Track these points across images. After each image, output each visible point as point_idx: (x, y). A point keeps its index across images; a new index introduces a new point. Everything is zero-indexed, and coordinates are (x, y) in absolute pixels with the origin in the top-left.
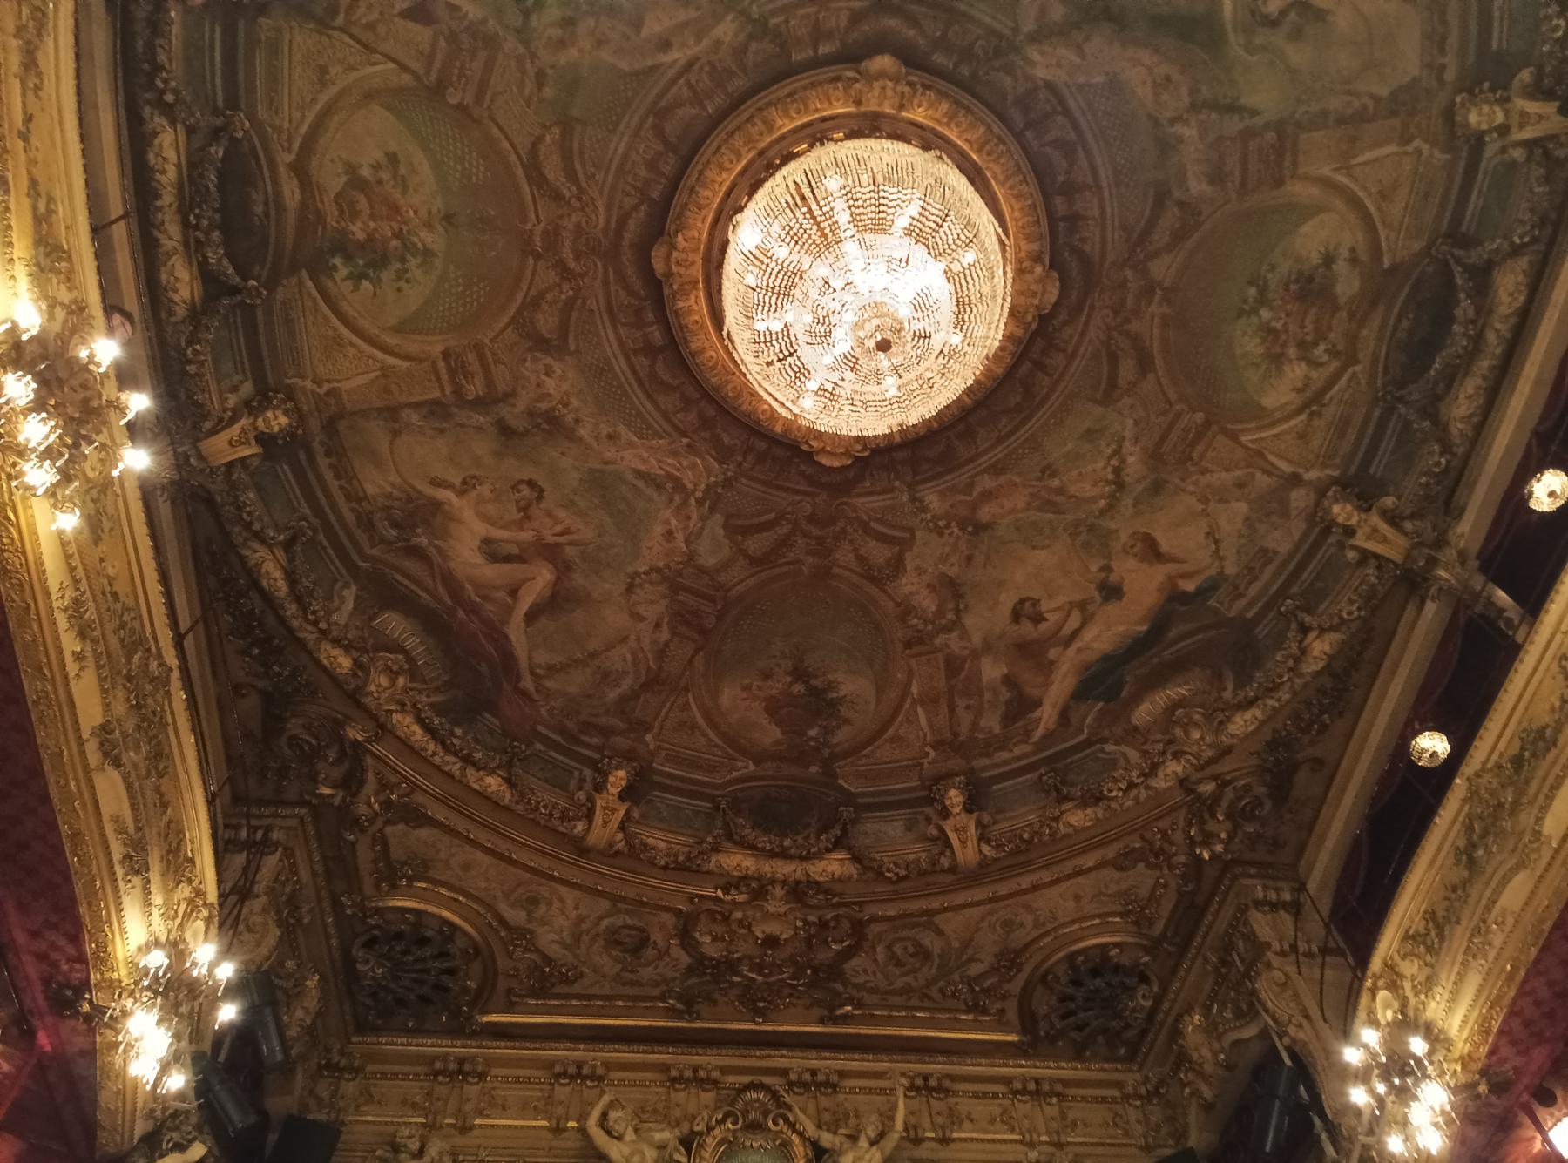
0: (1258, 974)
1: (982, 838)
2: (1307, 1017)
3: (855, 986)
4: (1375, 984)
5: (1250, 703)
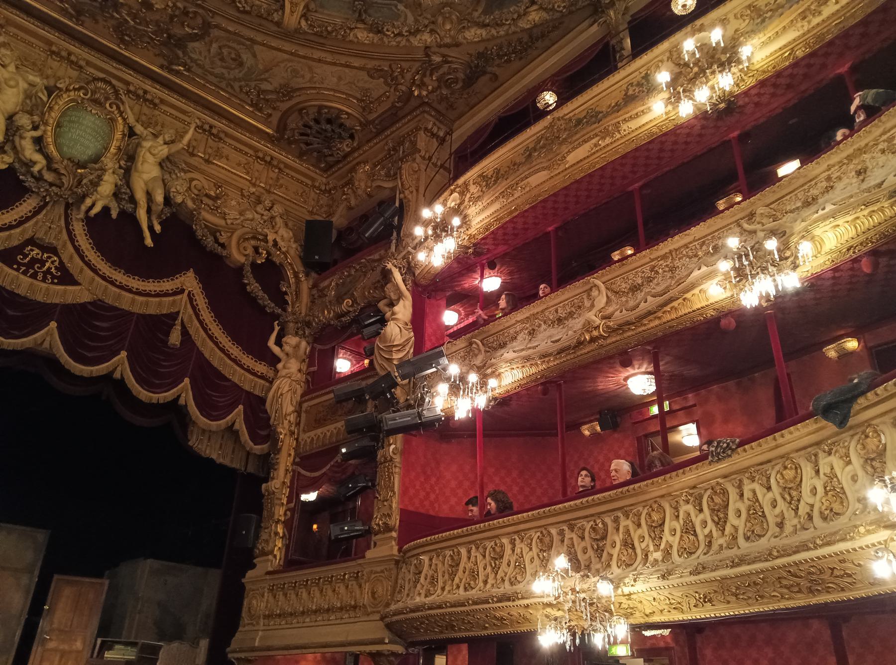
0: (407, 161)
1: (304, 16)
2: (417, 190)
3: (190, 58)
4: (455, 189)
5: (485, 26)
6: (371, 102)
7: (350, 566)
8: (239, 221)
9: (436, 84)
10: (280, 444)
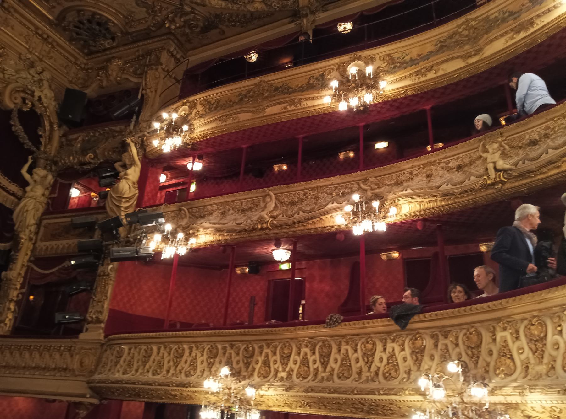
0: (152, 69)
2: (156, 91)
4: (186, 103)
6: (133, 21)
7: (68, 342)
8: (14, 78)
9: (182, 24)
10: (21, 246)
